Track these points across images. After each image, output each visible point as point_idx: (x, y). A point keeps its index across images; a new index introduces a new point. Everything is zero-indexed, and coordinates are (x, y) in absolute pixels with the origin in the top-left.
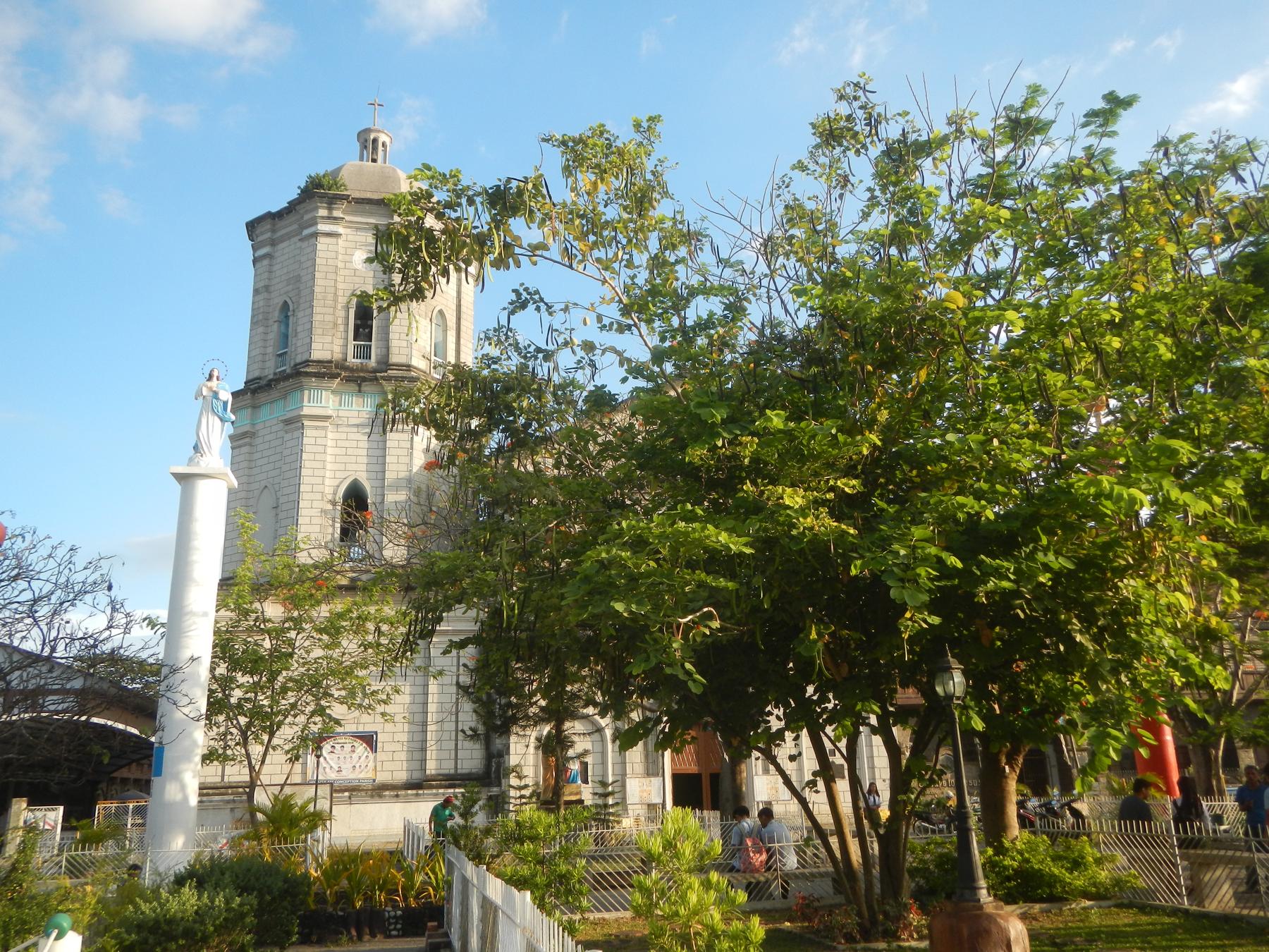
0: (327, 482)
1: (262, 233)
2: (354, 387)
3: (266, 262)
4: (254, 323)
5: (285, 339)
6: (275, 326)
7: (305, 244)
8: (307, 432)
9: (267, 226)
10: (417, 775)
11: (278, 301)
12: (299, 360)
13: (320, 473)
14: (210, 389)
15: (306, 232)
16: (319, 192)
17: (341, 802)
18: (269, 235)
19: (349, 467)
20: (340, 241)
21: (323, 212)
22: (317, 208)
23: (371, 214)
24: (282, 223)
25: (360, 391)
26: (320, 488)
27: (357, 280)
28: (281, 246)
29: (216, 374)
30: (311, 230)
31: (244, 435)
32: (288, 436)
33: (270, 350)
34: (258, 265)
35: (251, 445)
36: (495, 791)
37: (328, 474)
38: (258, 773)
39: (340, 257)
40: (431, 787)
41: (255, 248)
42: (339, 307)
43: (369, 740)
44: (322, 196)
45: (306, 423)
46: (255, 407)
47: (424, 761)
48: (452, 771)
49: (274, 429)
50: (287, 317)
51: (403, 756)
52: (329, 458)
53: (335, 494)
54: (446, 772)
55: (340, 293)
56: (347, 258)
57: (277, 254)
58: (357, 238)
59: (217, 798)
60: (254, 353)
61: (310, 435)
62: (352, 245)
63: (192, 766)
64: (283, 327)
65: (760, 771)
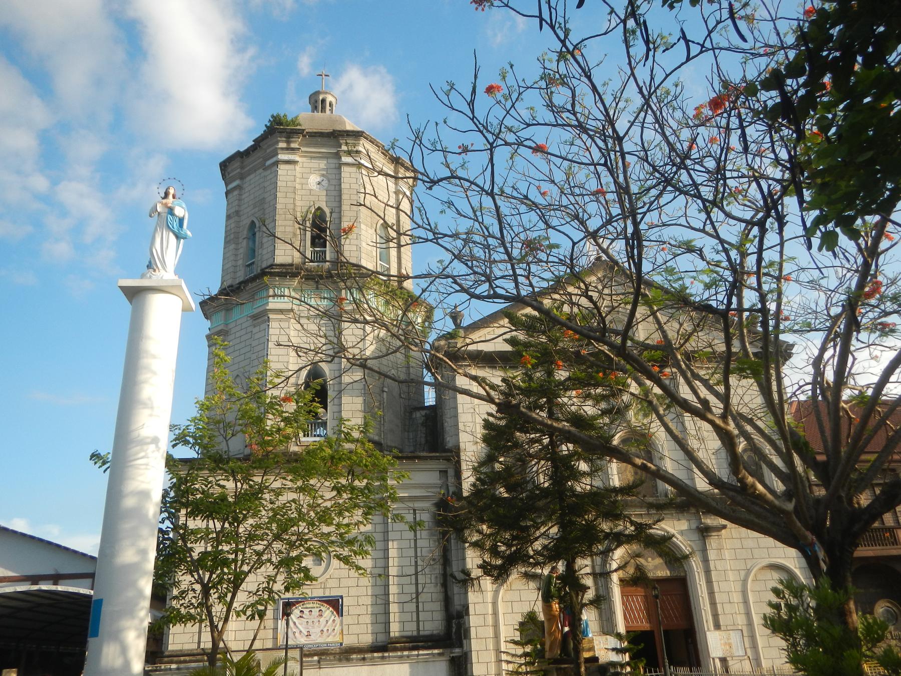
1: (233, 171)
3: (236, 193)
4: (227, 242)
5: (252, 252)
6: (245, 243)
7: (269, 172)
8: (273, 324)
9: (236, 164)
10: (382, 638)
11: (246, 222)
12: (264, 266)
14: (166, 205)
15: (269, 163)
16: (279, 130)
17: (311, 666)
18: (238, 170)
20: (298, 168)
21: (282, 145)
22: (277, 142)
23: (323, 146)
24: (251, 159)
25: (317, 288)
28: (248, 179)
29: (172, 191)
30: (274, 159)
31: (219, 333)
33: (240, 262)
34: (230, 196)
36: (457, 651)
38: (221, 633)
39: (298, 180)
40: (395, 649)
41: (227, 185)
43: (335, 604)
44: (282, 132)
45: (271, 316)
47: (387, 623)
48: (415, 633)
49: (244, 326)
50: (254, 234)
51: (368, 619)
54: (409, 634)
56: (304, 181)
57: (245, 186)
58: (311, 165)
59: (193, 665)
60: (227, 266)
62: (307, 170)
63: (136, 622)
64: (251, 243)
65: (712, 628)
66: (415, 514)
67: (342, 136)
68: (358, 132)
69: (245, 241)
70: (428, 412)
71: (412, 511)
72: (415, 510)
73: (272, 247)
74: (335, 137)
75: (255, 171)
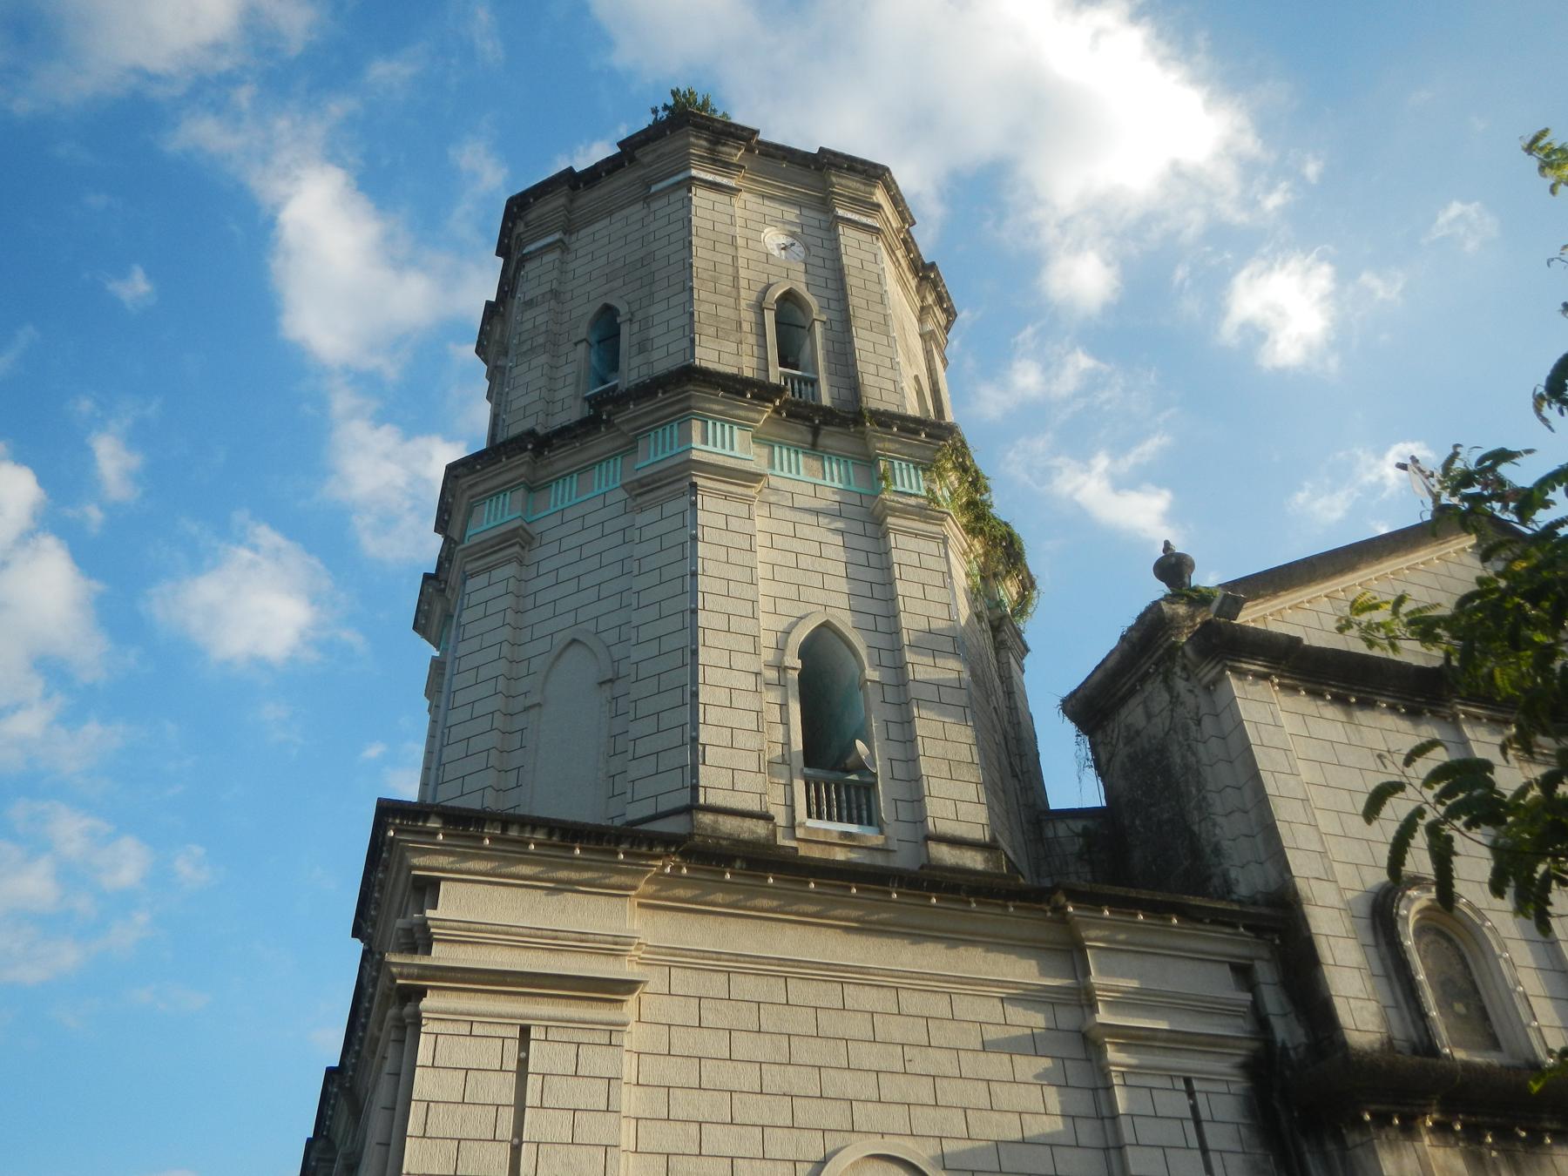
0: (765, 621)
2: (802, 432)
9: (558, 201)
13: (748, 592)
19: (807, 594)
25: (814, 446)
26: (748, 626)
27: (772, 270)
28: (582, 233)
30: (680, 177)
32: (641, 519)
33: (565, 392)
35: (521, 563)
37: (765, 604)
42: (743, 304)
46: (533, 487)
52: (762, 571)
53: (780, 649)
55: (743, 283)
56: (750, 234)
61: (712, 509)
66: (1191, 1093)
67: (839, 168)
68: (875, 166)
69: (582, 347)
70: (1089, 823)
71: (1181, 1085)
72: (1188, 1081)
73: (686, 343)
74: (819, 169)
75: (611, 213)
